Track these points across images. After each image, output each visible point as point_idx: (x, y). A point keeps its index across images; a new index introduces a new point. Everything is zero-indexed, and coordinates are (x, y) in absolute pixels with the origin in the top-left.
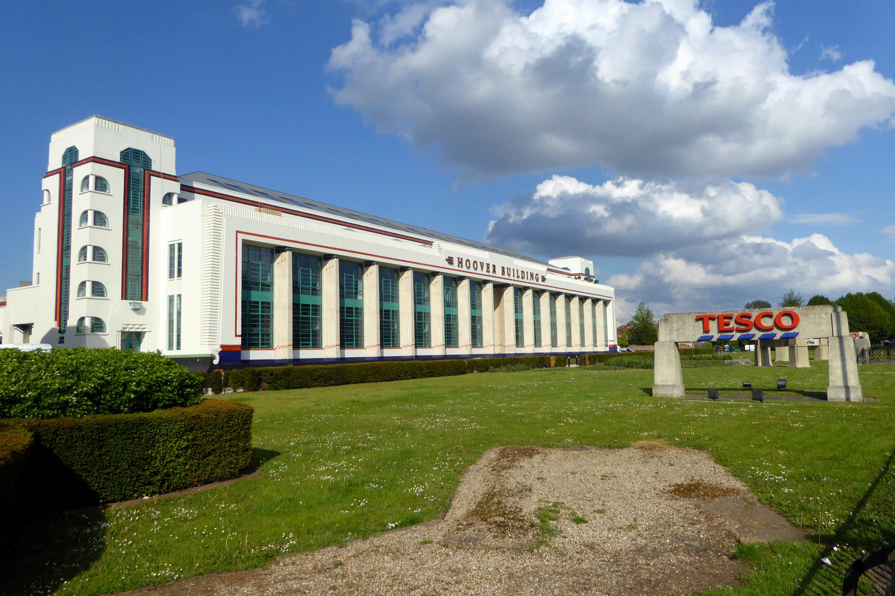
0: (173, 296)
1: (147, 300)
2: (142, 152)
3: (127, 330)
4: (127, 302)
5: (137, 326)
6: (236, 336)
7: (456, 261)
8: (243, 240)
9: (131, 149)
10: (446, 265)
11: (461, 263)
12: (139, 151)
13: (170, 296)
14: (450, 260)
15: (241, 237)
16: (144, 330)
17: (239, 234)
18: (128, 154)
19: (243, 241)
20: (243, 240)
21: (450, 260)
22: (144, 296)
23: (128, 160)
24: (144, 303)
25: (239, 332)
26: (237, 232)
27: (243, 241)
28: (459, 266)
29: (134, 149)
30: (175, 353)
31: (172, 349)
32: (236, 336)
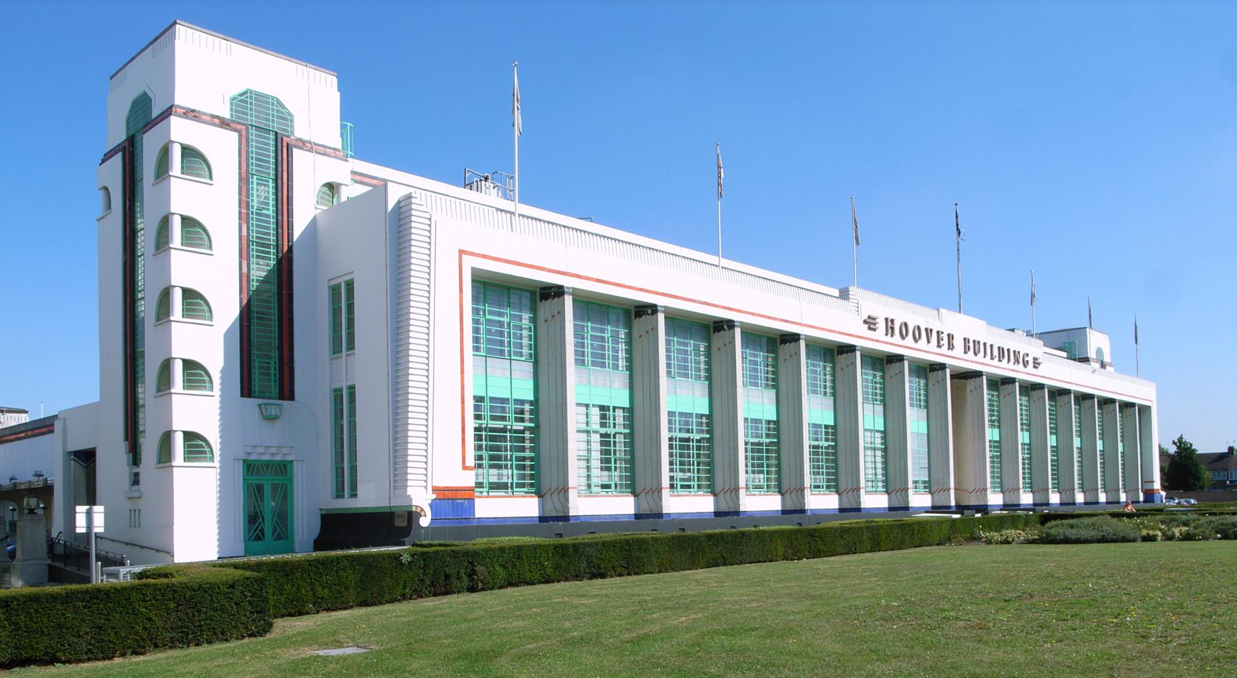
0: (341, 390)
1: (292, 398)
2: (273, 98)
3: (253, 457)
4: (252, 403)
5: (273, 450)
6: (465, 468)
7: (881, 325)
8: (472, 268)
9: (251, 93)
10: (863, 330)
11: (892, 329)
12: (267, 97)
13: (335, 391)
14: (870, 323)
15: (470, 263)
16: (289, 458)
17: (464, 256)
18: (247, 102)
19: (473, 269)
20: (472, 268)
21: (870, 323)
22: (286, 391)
23: (246, 114)
24: (286, 403)
25: (471, 462)
26: (461, 252)
27: (473, 269)
28: (887, 334)
29: (258, 94)
30: (347, 504)
31: (343, 496)
32: (465, 468)
